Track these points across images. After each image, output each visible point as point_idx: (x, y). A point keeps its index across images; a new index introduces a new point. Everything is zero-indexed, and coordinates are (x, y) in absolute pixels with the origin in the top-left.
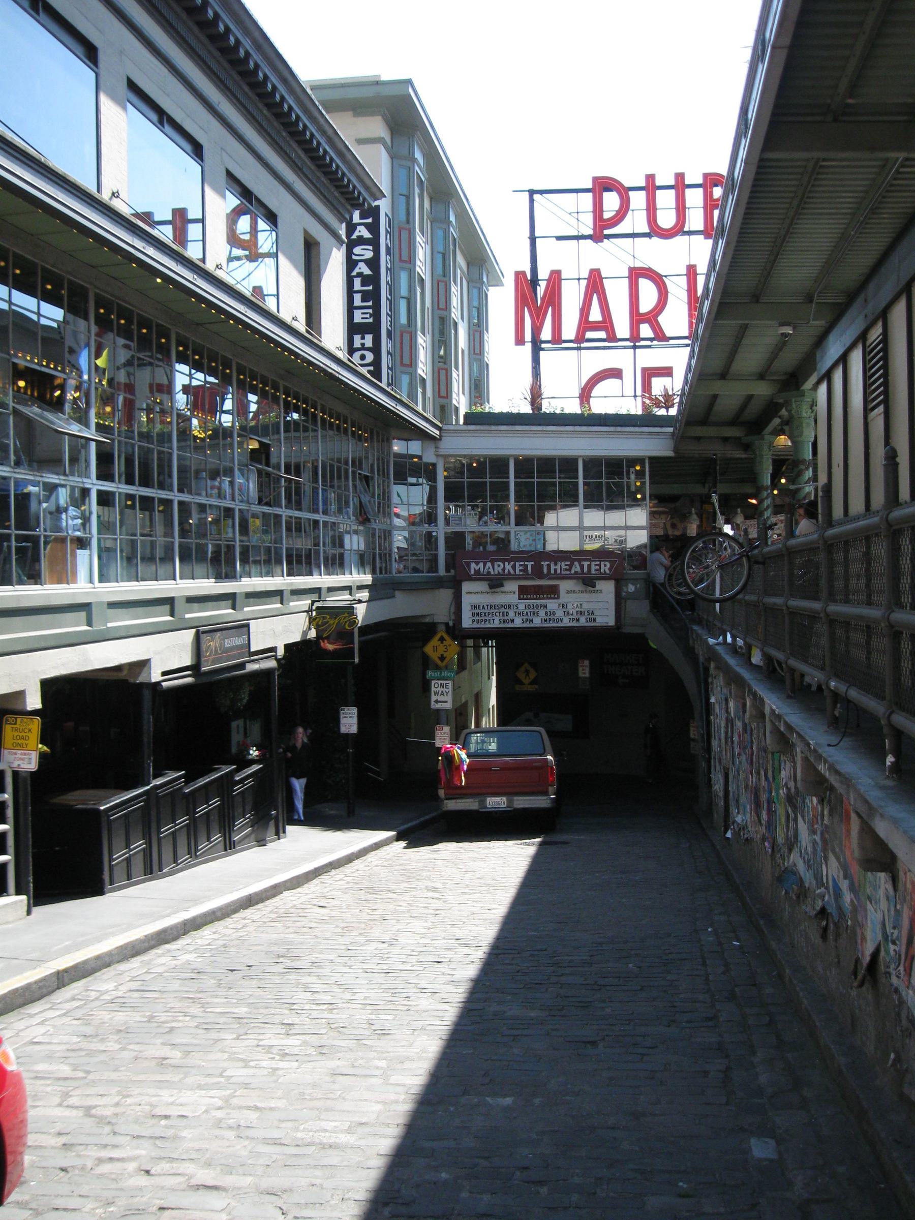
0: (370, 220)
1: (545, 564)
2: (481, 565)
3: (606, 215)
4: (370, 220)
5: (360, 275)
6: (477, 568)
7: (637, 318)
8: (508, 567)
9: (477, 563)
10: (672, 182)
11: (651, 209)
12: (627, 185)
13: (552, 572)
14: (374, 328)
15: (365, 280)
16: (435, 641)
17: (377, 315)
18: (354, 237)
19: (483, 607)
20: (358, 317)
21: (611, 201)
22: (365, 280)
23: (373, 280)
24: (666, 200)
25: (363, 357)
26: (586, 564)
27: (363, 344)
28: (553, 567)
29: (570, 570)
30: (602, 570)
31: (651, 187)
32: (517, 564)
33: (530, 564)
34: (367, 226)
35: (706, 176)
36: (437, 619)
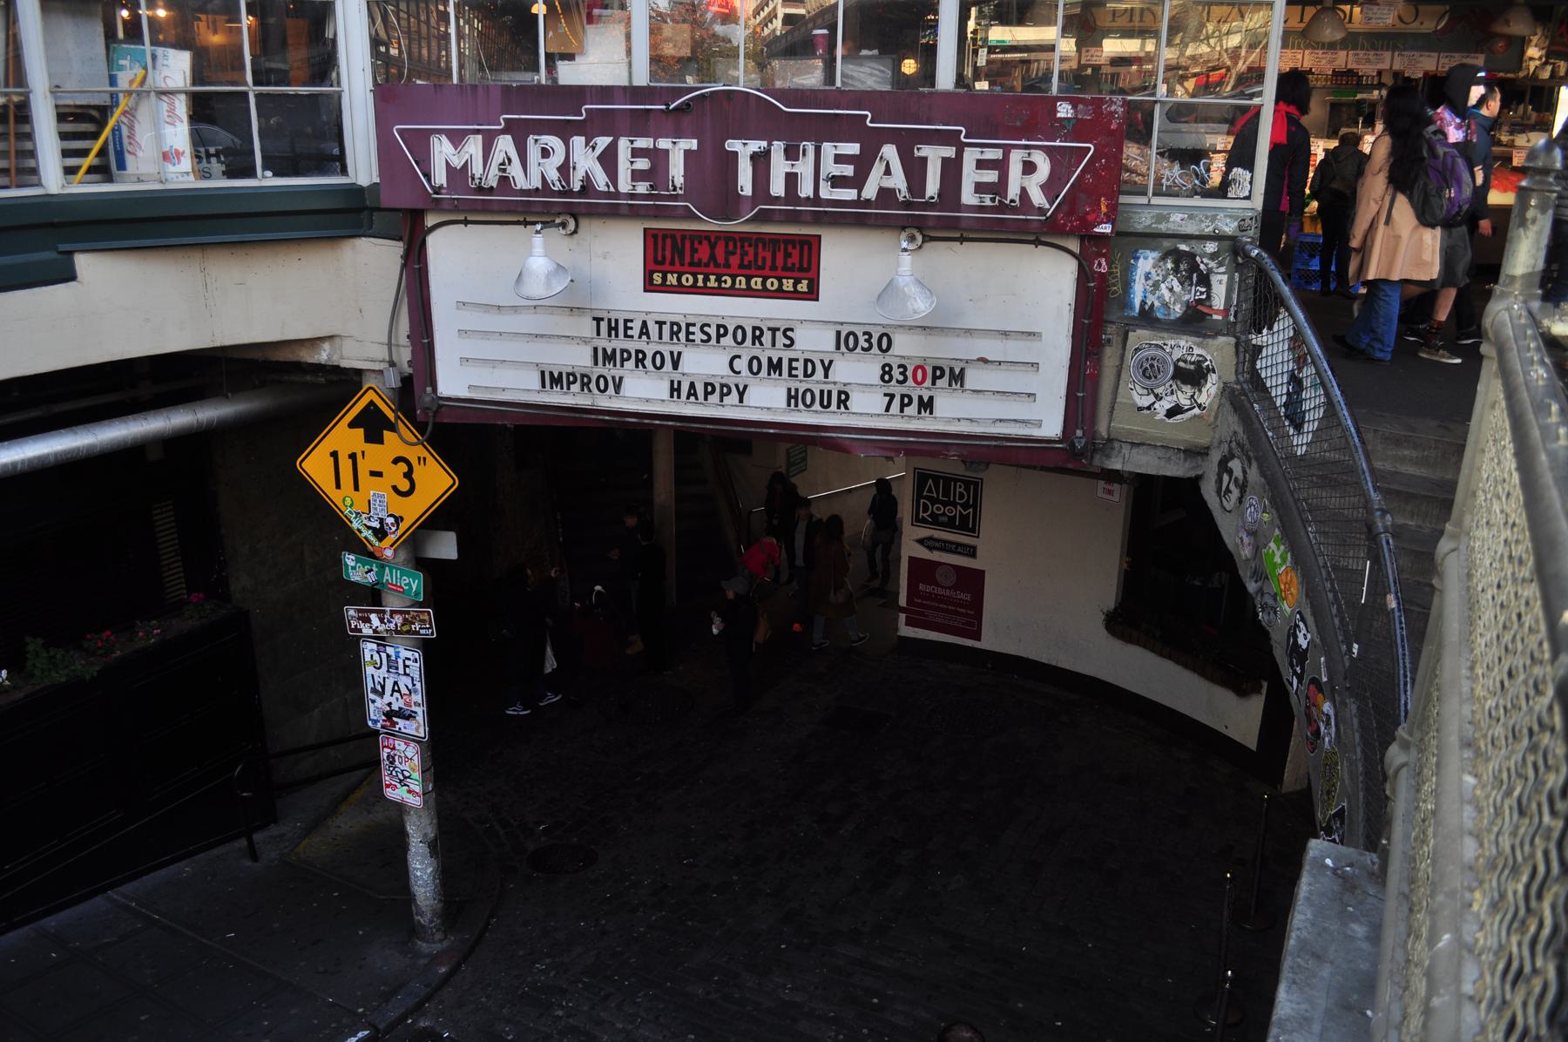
1: (744, 149)
2: (474, 146)
6: (457, 163)
8: (586, 161)
9: (457, 139)
13: (778, 188)
16: (342, 436)
19: (644, 330)
26: (934, 155)
28: (779, 167)
29: (858, 181)
30: (1013, 192)
32: (624, 145)
33: (678, 150)
36: (350, 356)
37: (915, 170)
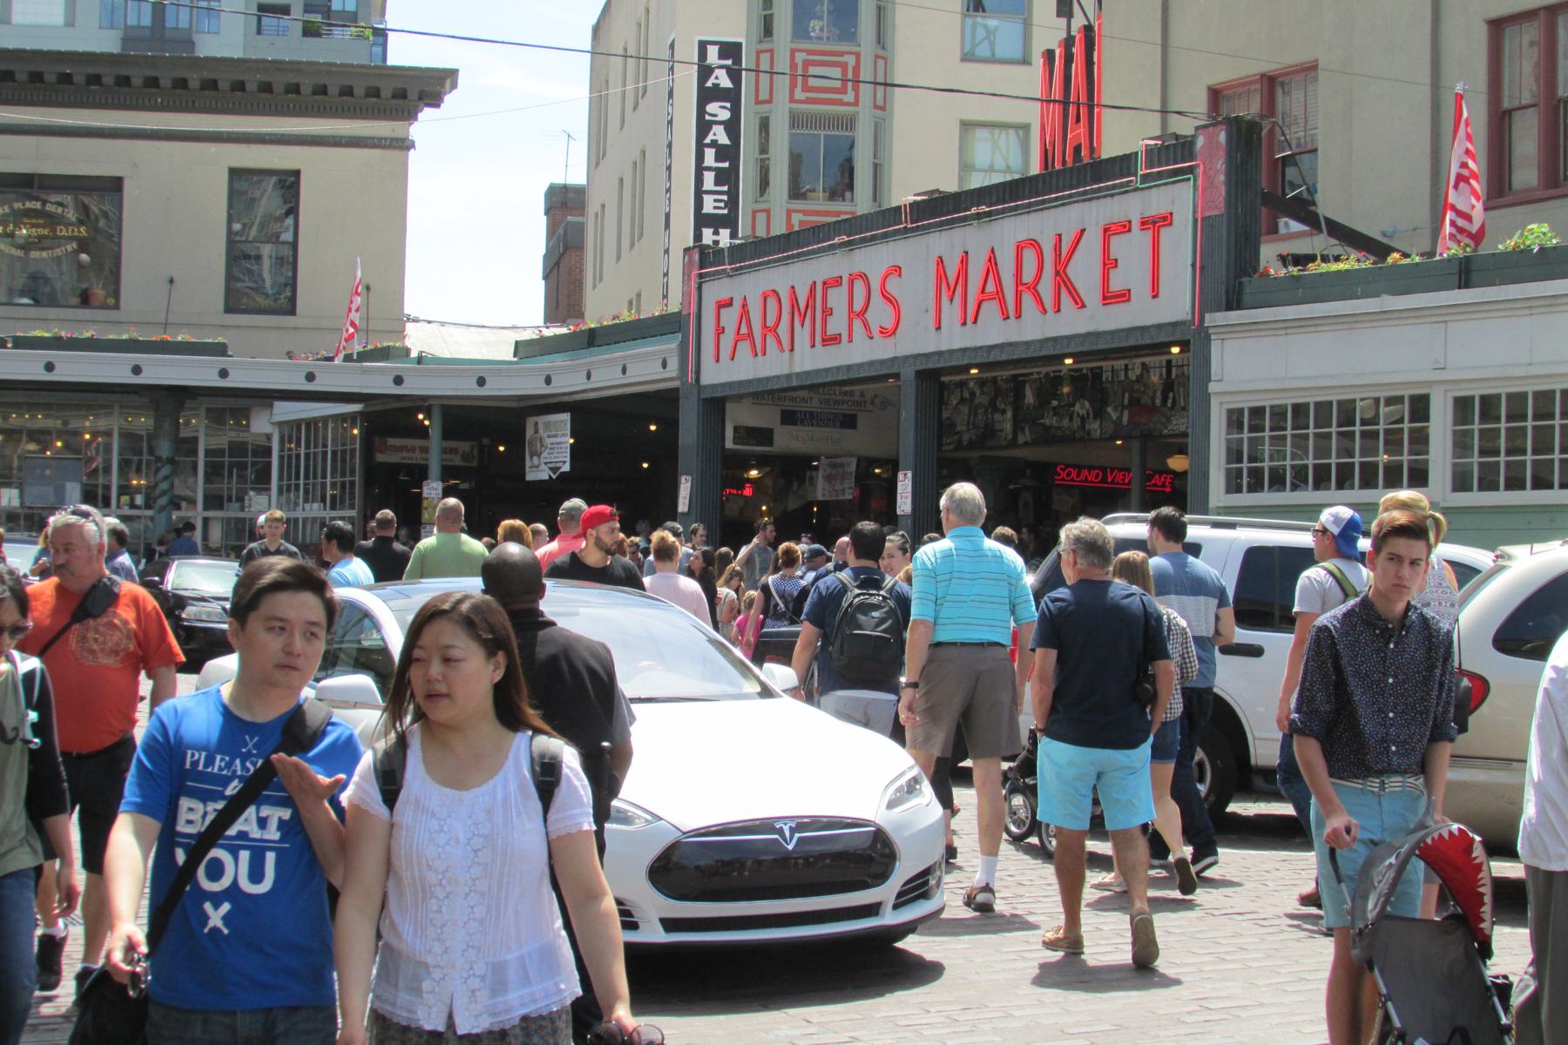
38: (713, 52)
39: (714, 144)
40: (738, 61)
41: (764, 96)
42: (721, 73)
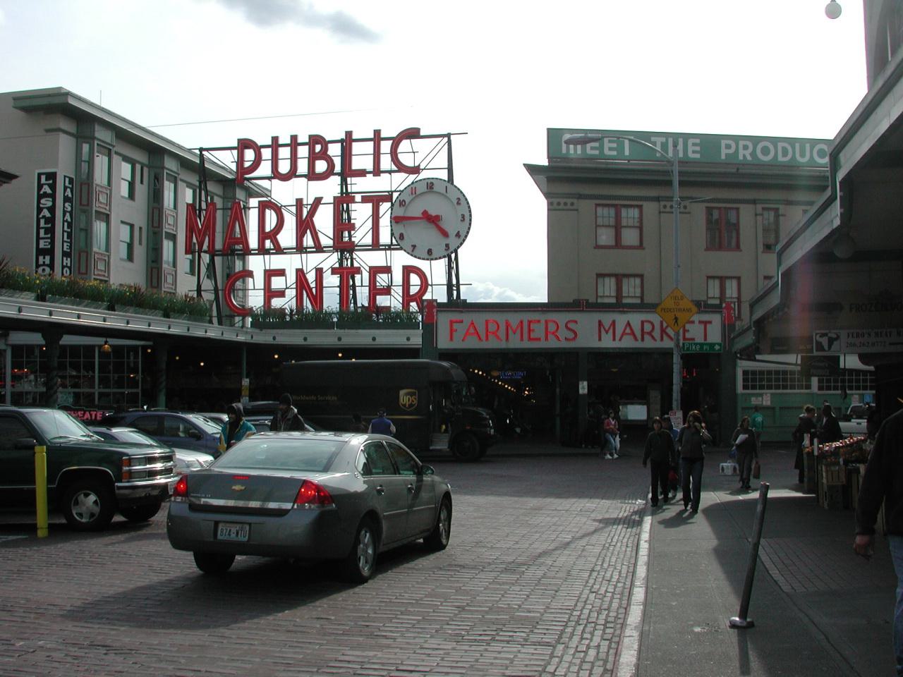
0: (51, 182)
3: (247, 165)
4: (51, 182)
5: (44, 217)
7: (263, 235)
10: (288, 141)
11: (275, 160)
12: (259, 144)
14: (50, 252)
15: (47, 220)
17: (53, 243)
18: (41, 192)
20: (42, 245)
21: (249, 155)
22: (47, 220)
23: (51, 220)
24: (284, 153)
25: (44, 270)
26: (94, 413)
27: (44, 262)
31: (275, 144)
34: (48, 185)
35: (310, 137)
37: (91, 415)
38: (67, 180)
39: (67, 221)
40: (55, 182)
41: (84, 202)
42: (69, 190)
